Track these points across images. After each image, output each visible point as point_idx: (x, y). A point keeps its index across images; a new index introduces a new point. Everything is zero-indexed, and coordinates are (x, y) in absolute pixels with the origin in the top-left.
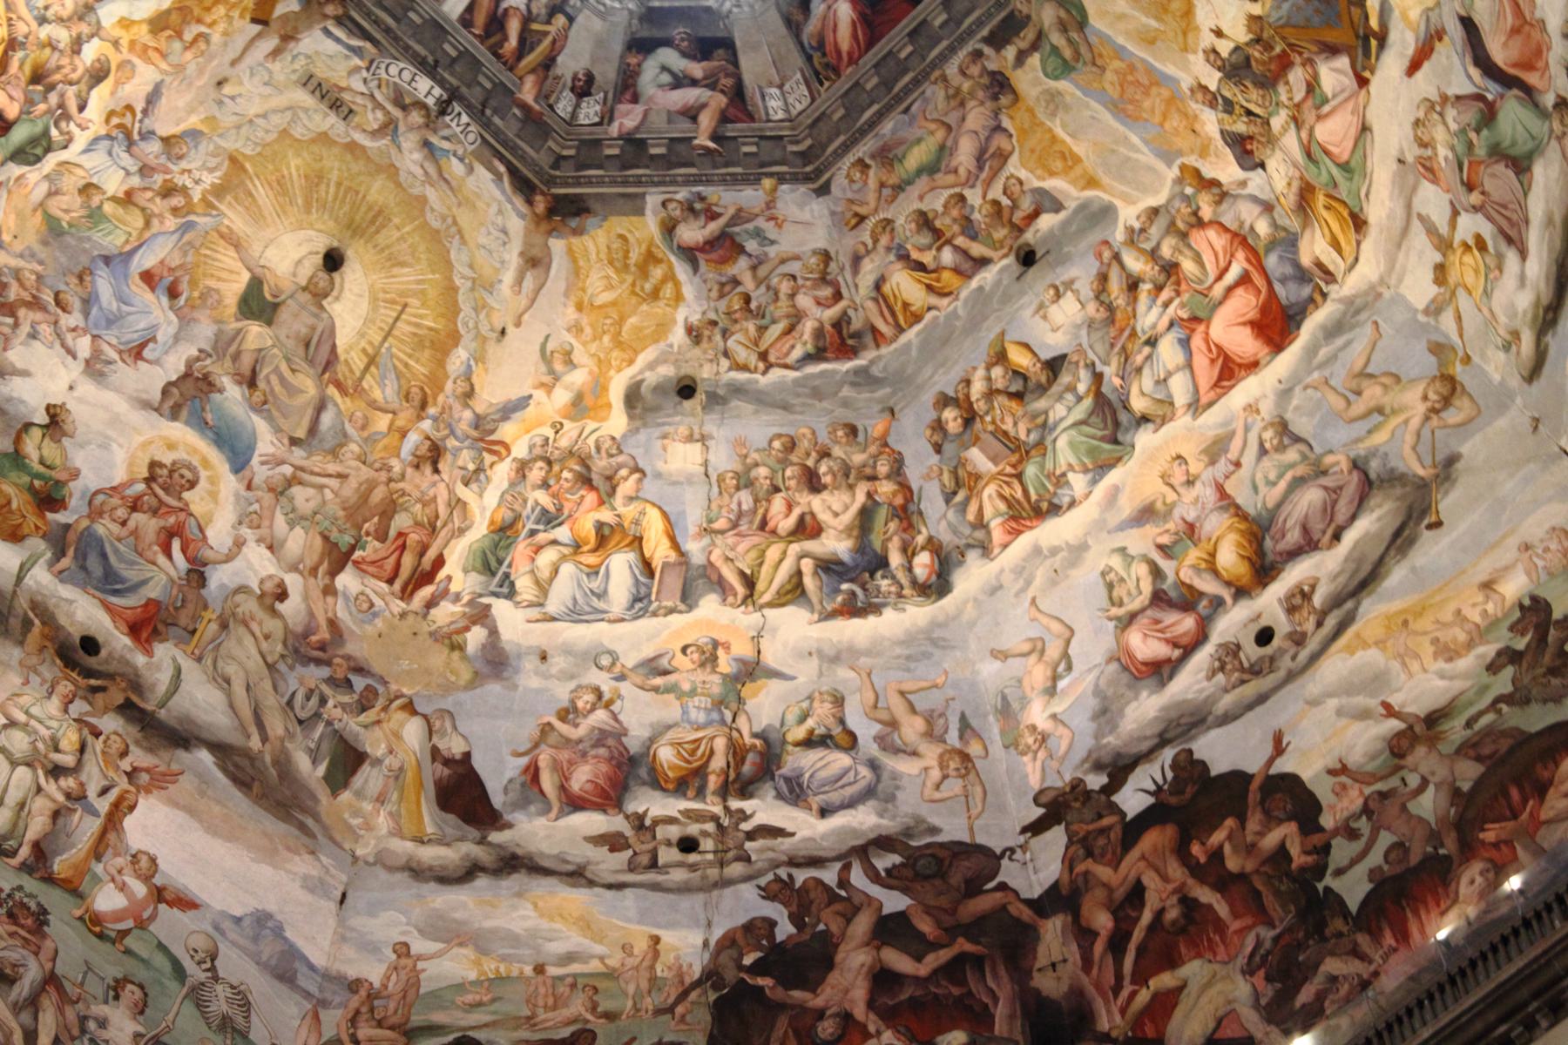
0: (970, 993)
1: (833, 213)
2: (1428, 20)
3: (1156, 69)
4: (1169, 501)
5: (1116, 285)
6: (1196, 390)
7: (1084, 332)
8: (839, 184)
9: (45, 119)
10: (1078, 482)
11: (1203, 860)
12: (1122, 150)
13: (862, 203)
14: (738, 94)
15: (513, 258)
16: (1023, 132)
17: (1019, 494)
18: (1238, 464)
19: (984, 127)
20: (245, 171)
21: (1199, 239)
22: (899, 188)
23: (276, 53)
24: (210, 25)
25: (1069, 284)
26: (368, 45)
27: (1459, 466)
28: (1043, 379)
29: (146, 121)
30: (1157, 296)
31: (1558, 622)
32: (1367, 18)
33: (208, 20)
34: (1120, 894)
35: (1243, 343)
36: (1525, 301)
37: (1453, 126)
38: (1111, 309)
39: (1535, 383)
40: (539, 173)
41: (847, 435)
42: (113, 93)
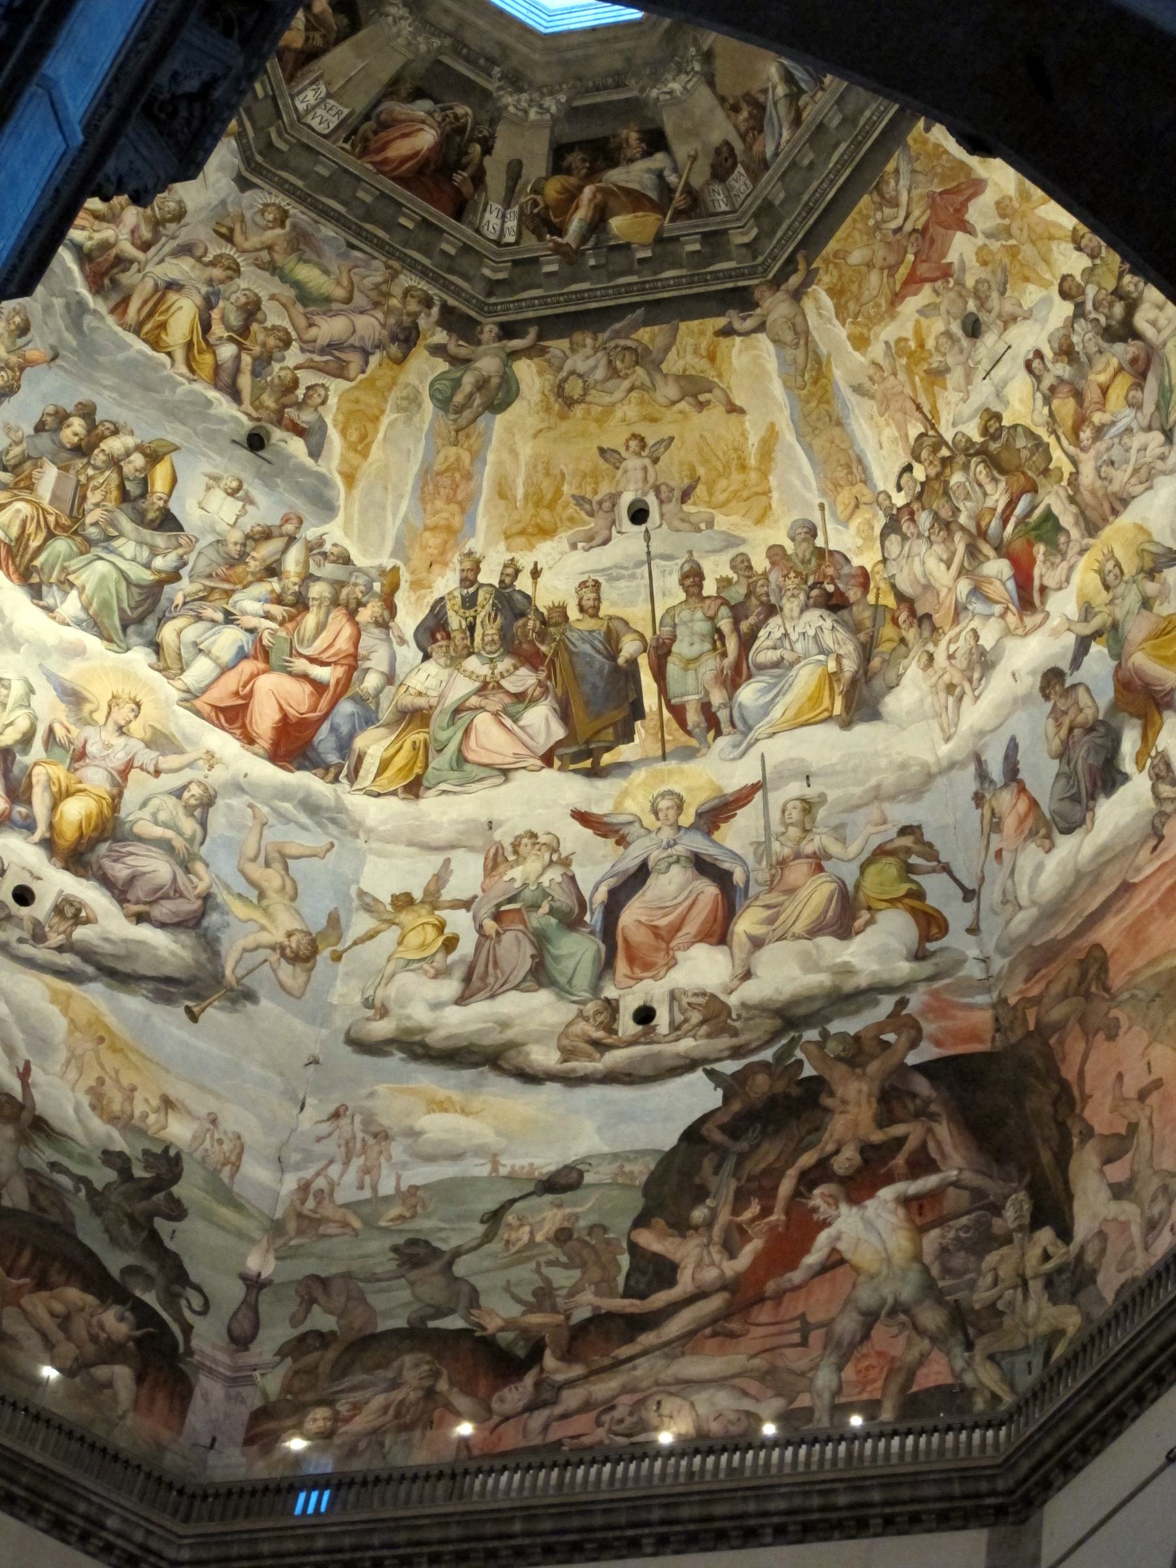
1: (223, 203)
2: (631, 823)
4: (96, 716)
5: (266, 551)
6: (205, 690)
7: (211, 538)
8: (257, 198)
10: (71, 605)
12: (390, 498)
13: (244, 233)
14: (309, 56)
16: (371, 382)
17: (34, 544)
18: (157, 773)
19: (362, 338)
21: (338, 618)
22: (273, 268)
25: (249, 500)
27: (250, 1007)
28: (151, 515)
30: (272, 602)
31: (171, 1194)
32: (608, 749)
35: (264, 718)
36: (420, 1014)
37: (545, 881)
38: (243, 556)
39: (348, 1049)
41: (18, 327)
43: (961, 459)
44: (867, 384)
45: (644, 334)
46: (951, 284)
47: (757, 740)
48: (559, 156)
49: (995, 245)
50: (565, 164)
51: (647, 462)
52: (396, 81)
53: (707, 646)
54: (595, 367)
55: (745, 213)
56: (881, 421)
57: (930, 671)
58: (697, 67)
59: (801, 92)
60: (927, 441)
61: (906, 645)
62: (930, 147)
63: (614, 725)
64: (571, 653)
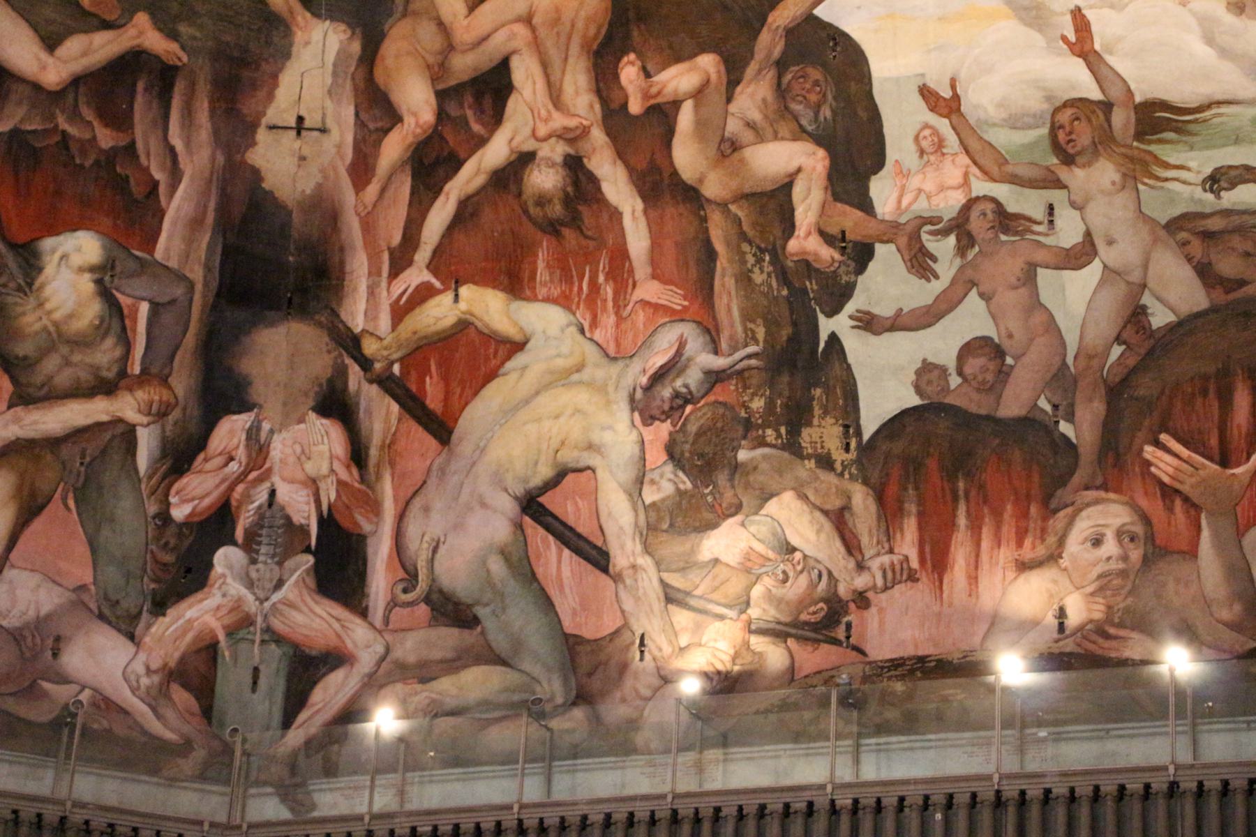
0: (131, 149)
11: (635, 107)
34: (464, 65)
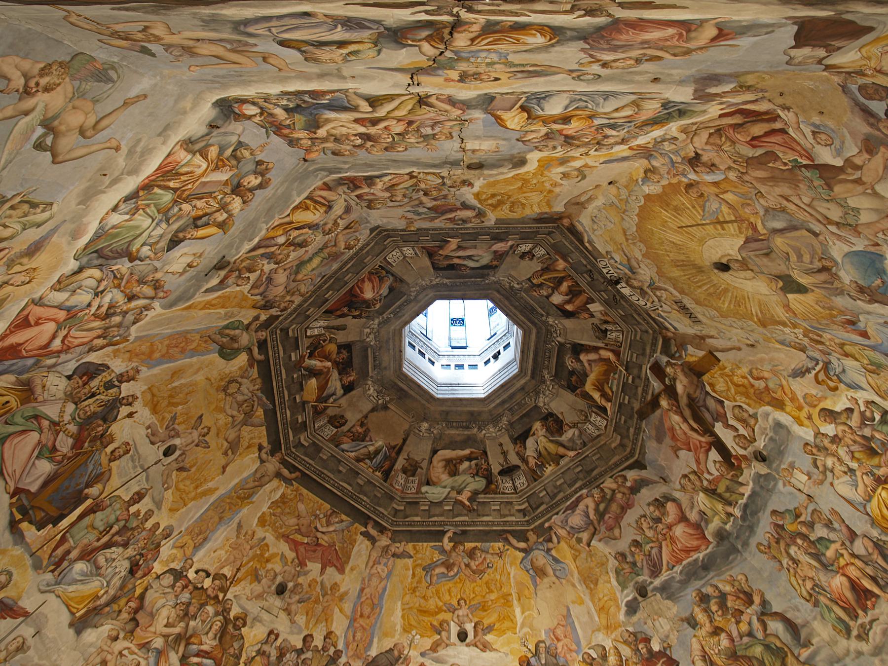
1: (368, 222)
3: (167, 363)
8: (363, 235)
9: (880, 428)
15: (591, 208)
20: (759, 320)
23: (712, 337)
24: (746, 378)
26: (653, 316)
29: (810, 366)
32: (31, 522)
33: (746, 381)
38: (145, 283)
40: (562, 233)
42: (826, 398)
43: (220, 609)
44: (243, 532)
45: (260, 412)
46: (298, 569)
47: (54, 592)
48: (347, 347)
49: (318, 589)
50: (342, 350)
51: (197, 441)
52: (402, 281)
53: (101, 529)
54: (244, 395)
55: (314, 437)
56: (227, 547)
57: (109, 642)
58: (380, 402)
59: (371, 460)
60: (224, 582)
61: (118, 615)
62: (354, 537)
63: (47, 514)
64: (85, 463)
